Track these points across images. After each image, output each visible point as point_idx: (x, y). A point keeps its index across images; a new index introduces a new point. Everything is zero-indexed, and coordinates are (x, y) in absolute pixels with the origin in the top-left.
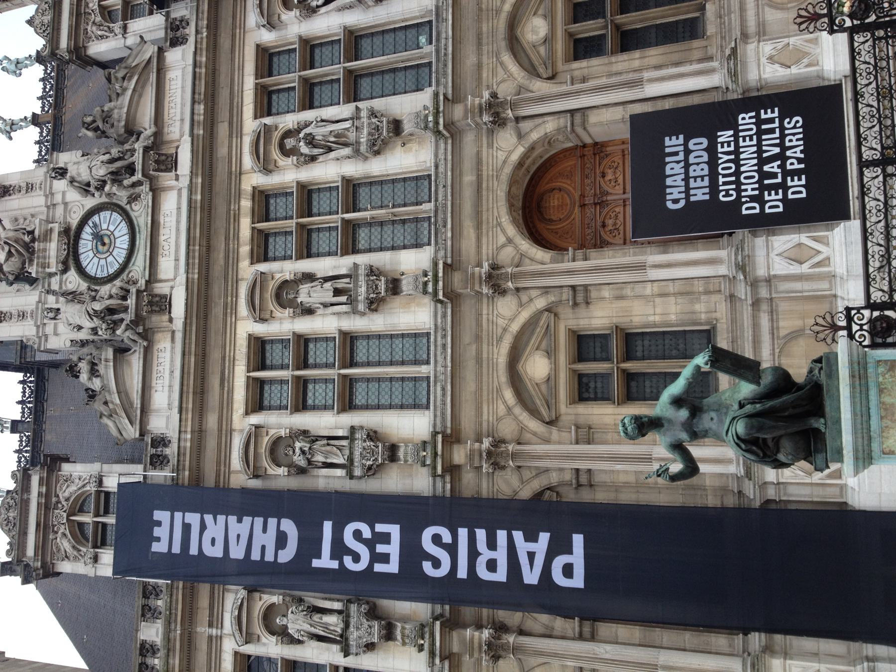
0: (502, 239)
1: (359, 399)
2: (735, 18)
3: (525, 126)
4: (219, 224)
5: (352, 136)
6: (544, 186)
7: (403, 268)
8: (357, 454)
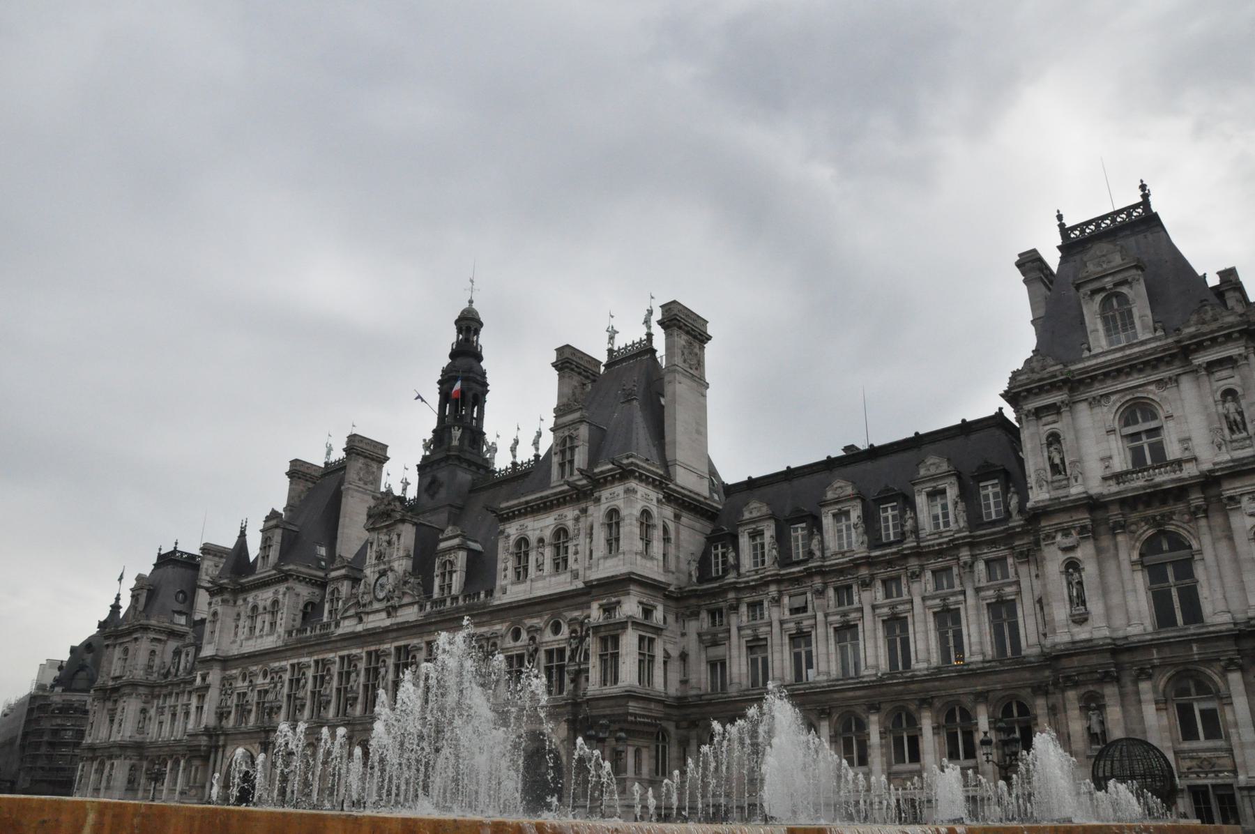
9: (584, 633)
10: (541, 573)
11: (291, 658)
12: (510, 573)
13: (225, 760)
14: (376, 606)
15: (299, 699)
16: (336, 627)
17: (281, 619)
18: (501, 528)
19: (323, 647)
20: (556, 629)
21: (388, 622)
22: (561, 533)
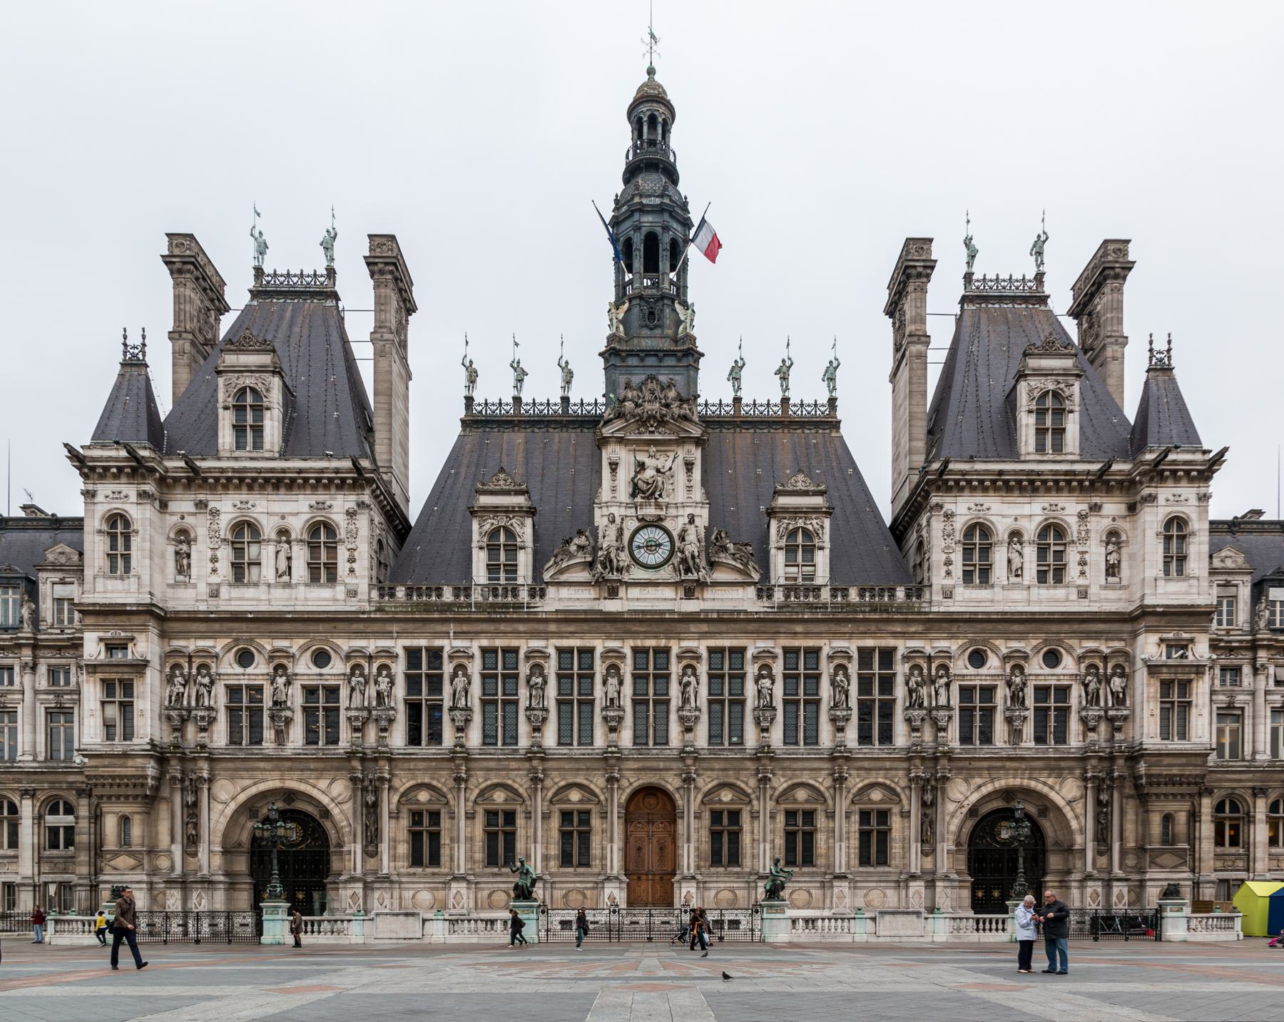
0: (632, 780)
1: (563, 707)
2: (714, 879)
3: (682, 791)
4: (654, 628)
5: (687, 707)
6: (660, 795)
7: (623, 732)
8: (535, 712)
9: (1109, 671)
10: (1013, 580)
11: (401, 634)
12: (957, 569)
13: (217, 807)
14: (638, 574)
15: (462, 709)
16: (532, 596)
17: (352, 560)
18: (934, 500)
19: (503, 627)
20: (1052, 658)
21: (691, 606)
22: (1053, 531)
